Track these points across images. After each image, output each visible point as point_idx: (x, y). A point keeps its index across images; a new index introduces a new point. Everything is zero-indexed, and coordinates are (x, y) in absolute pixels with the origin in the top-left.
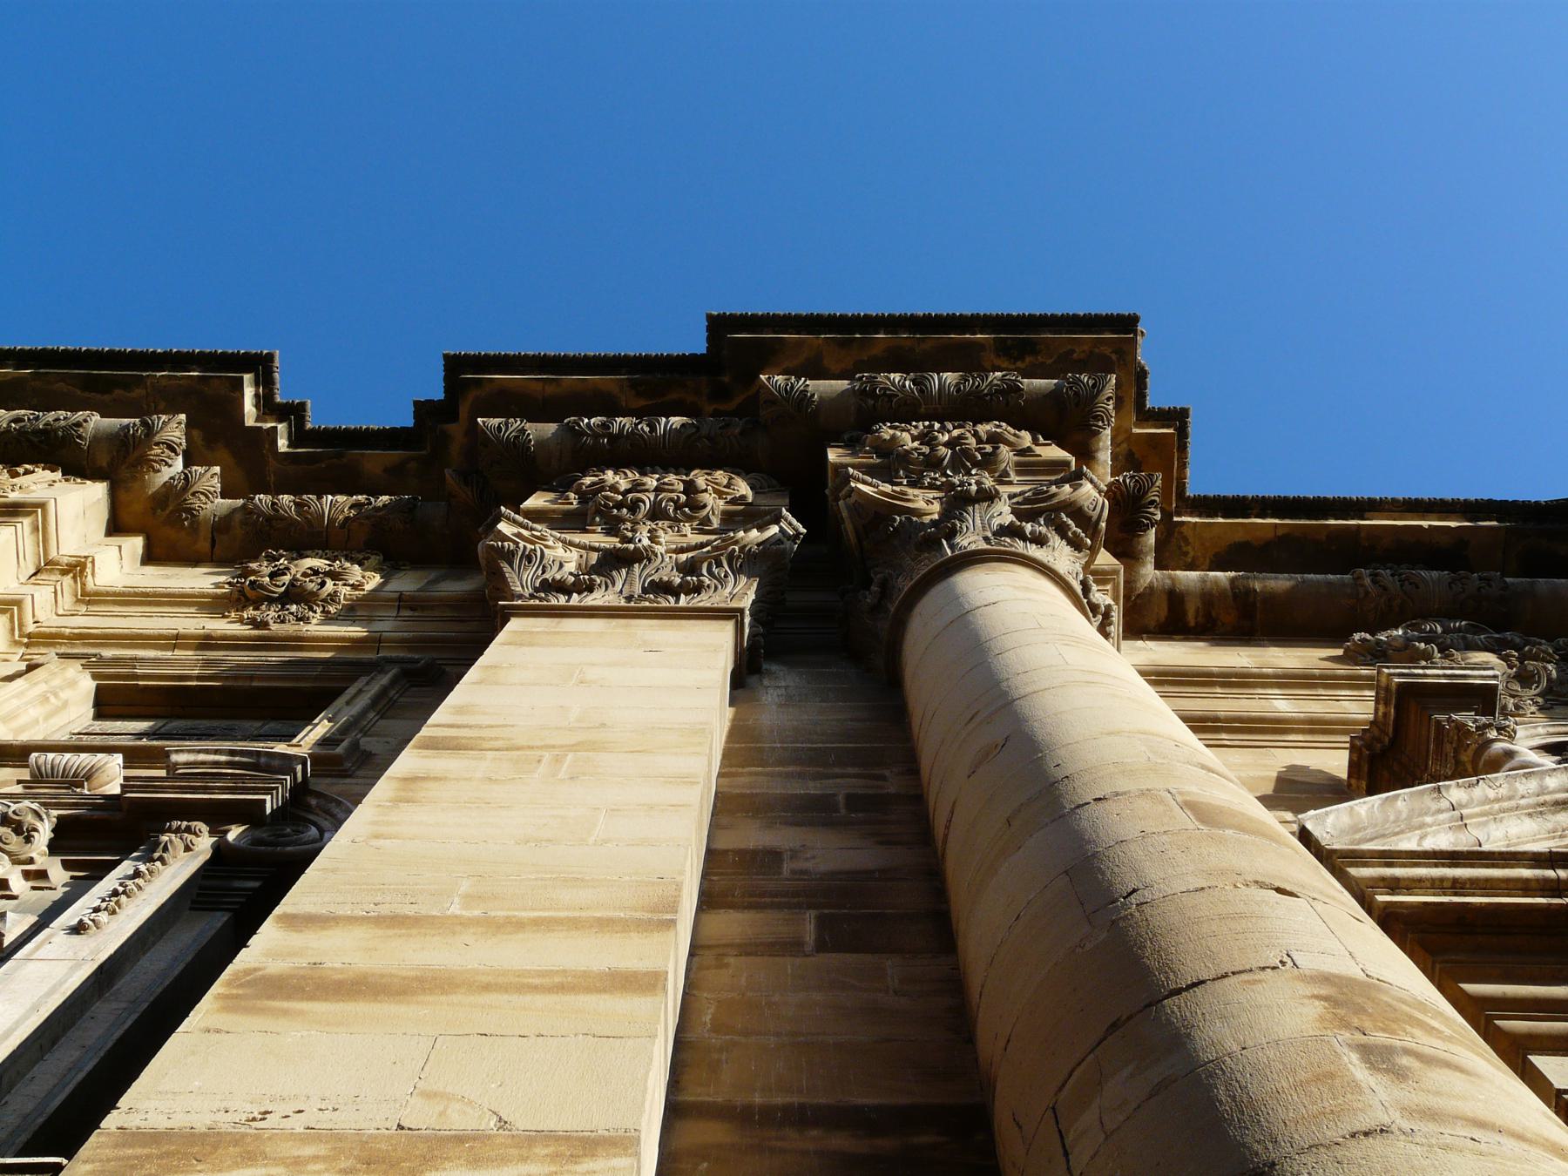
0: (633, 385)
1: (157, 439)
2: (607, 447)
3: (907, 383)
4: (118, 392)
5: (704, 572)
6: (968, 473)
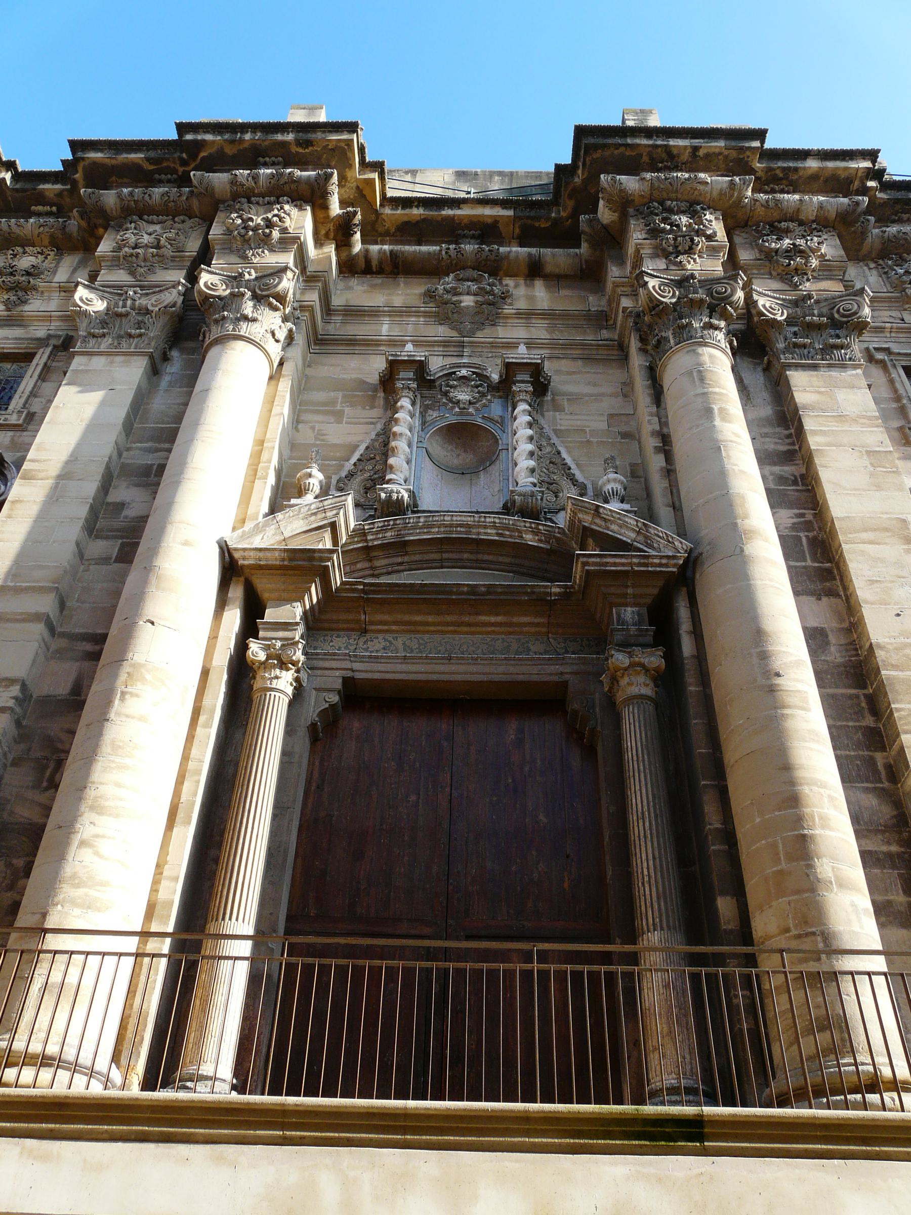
0: (148, 159)
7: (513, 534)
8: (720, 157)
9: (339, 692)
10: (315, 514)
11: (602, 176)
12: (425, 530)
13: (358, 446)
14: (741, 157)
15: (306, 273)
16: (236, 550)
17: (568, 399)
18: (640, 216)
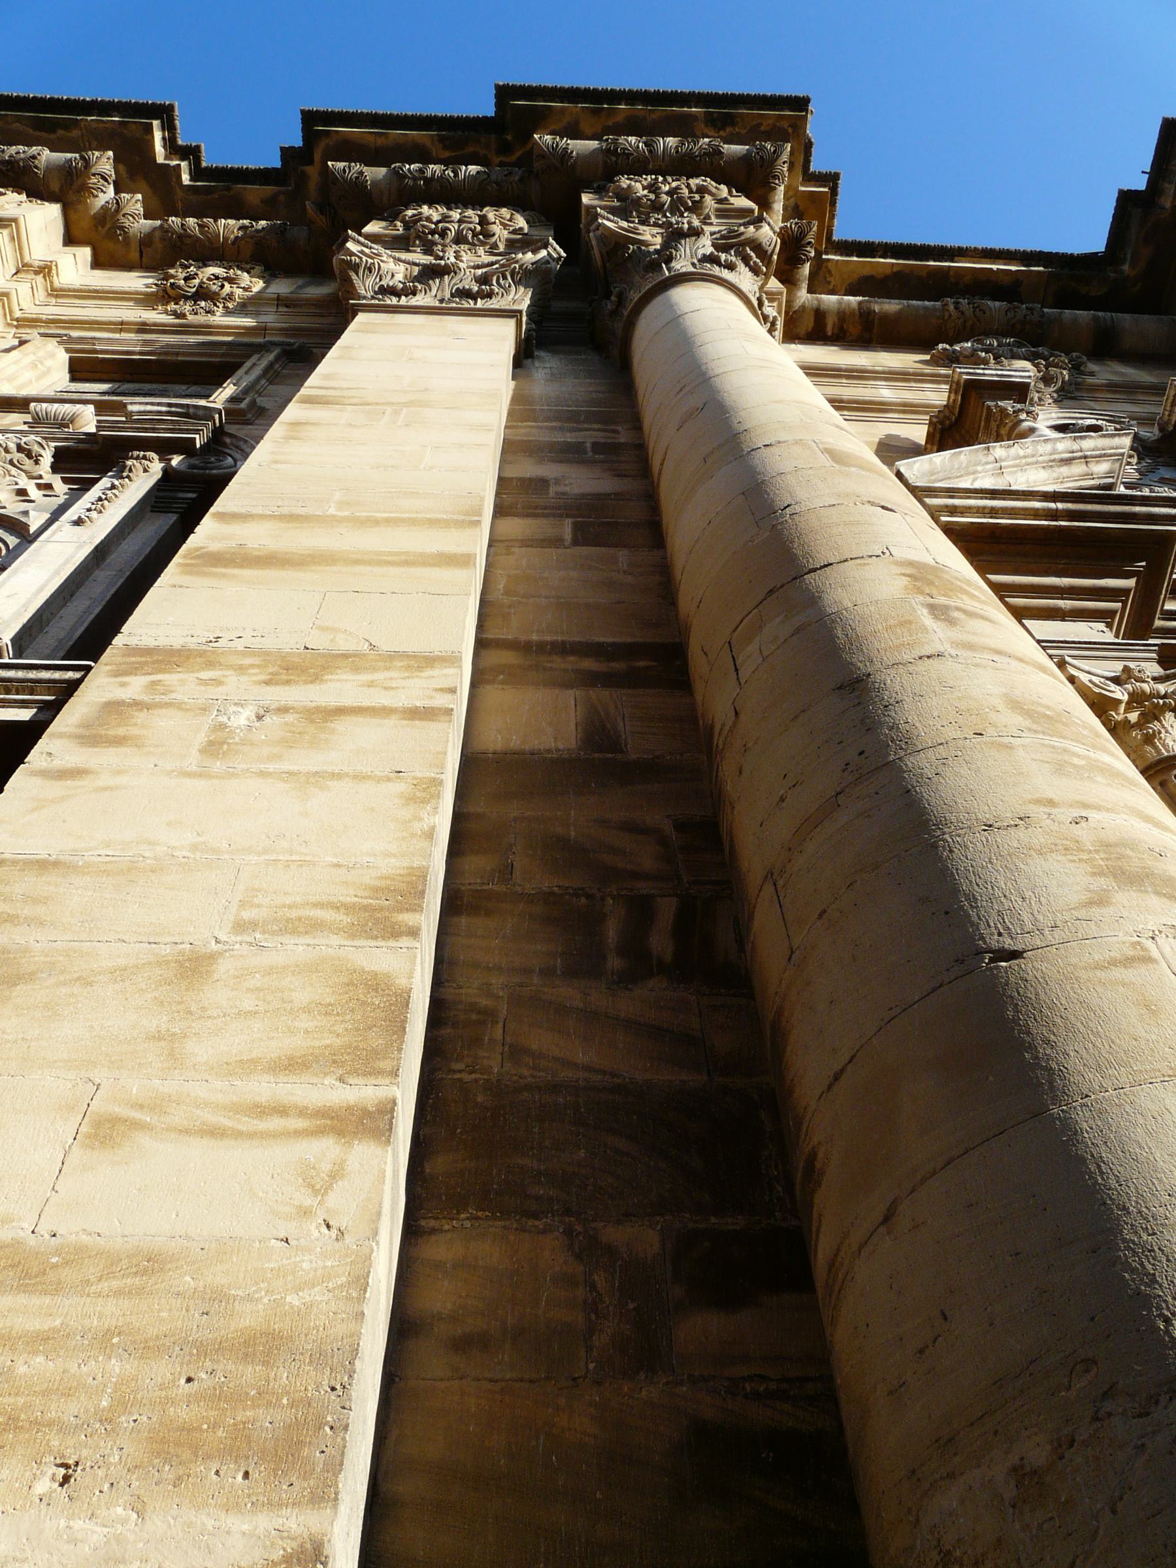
1: (93, 171)
2: (423, 187)
3: (640, 145)
4: (61, 132)
5: (494, 283)
6: (682, 216)
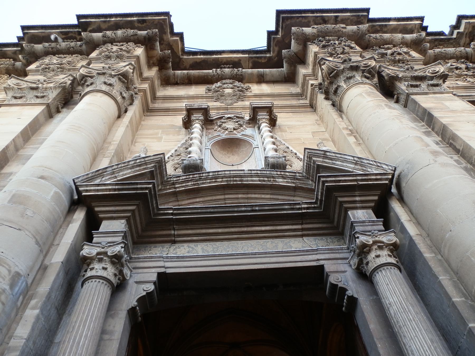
7: (269, 179)
8: (349, 21)
9: (155, 283)
10: (140, 166)
11: (293, 28)
12: (213, 180)
13: (171, 151)
14: (359, 20)
15: (142, 76)
16: (81, 186)
17: (288, 127)
18: (314, 44)
